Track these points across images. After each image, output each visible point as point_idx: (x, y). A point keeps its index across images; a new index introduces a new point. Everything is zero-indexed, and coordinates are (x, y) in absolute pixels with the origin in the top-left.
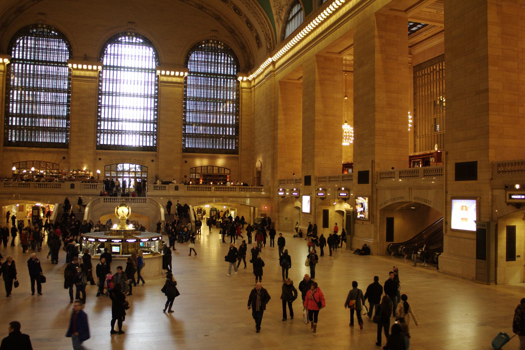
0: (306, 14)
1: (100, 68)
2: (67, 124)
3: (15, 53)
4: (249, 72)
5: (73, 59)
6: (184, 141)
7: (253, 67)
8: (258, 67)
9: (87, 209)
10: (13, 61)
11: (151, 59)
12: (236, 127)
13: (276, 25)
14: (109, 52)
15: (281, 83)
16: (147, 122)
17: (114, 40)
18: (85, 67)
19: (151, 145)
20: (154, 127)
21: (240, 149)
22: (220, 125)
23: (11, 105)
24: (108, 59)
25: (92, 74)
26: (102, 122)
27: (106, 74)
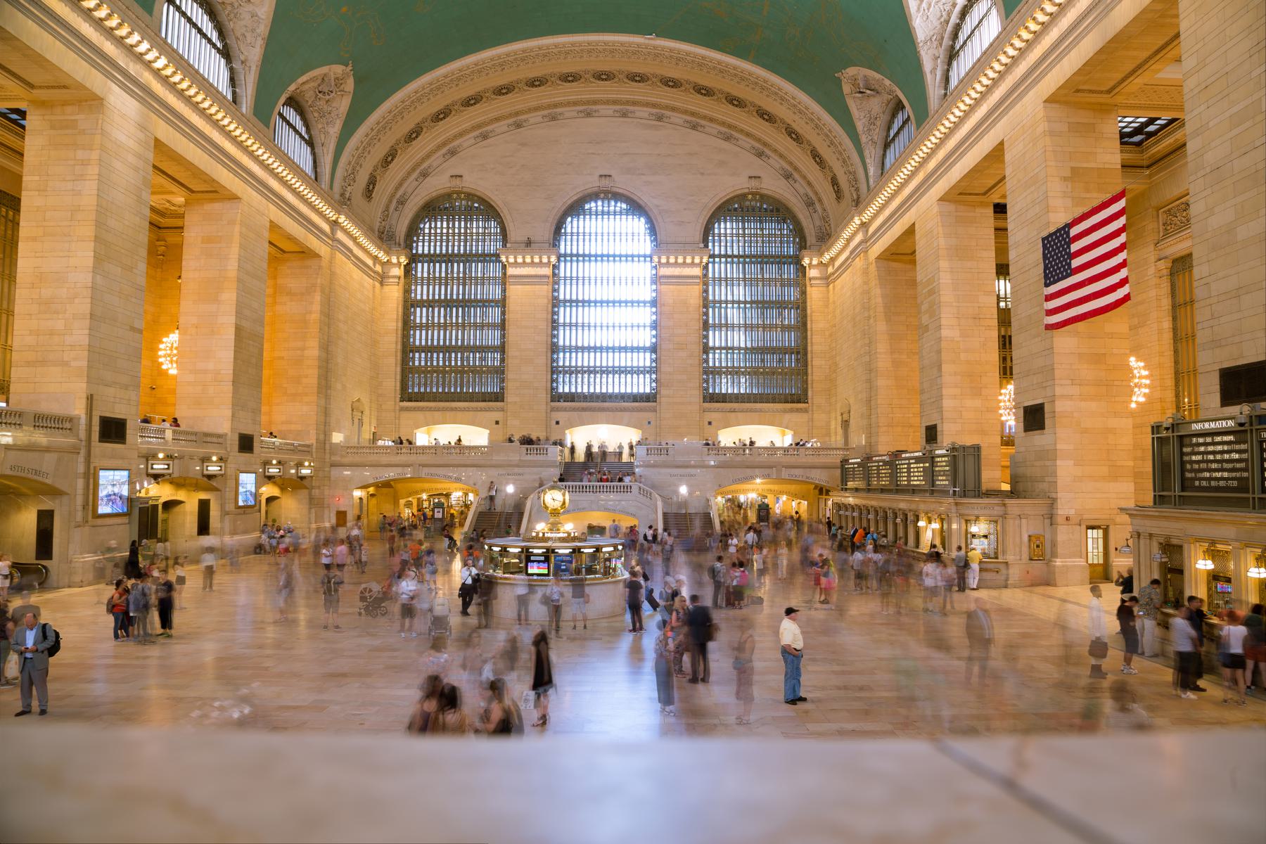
0: (919, 125)
2: (503, 360)
6: (707, 381)
7: (829, 235)
8: (837, 239)
10: (414, 259)
11: (642, 238)
13: (867, 153)
14: (569, 230)
15: (878, 258)
17: (576, 208)
19: (648, 390)
21: (810, 393)
24: (569, 243)
26: (561, 355)
27: (565, 269)
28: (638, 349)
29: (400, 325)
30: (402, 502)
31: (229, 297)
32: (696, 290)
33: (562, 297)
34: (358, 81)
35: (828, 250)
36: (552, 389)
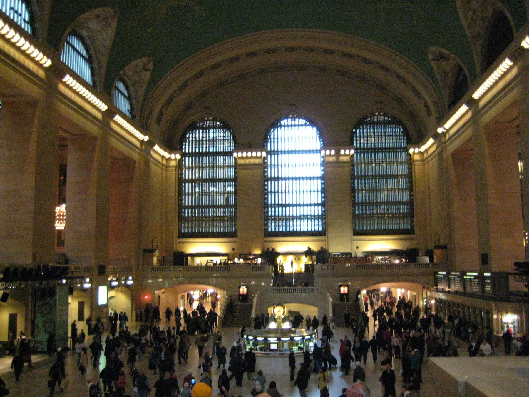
1: (264, 154)
3: (185, 148)
4: (421, 143)
5: (238, 147)
9: (255, 300)
10: (184, 155)
12: (411, 203)
16: (314, 205)
17: (276, 125)
18: (249, 154)
20: (322, 211)
22: (392, 203)
23: (183, 197)
24: (272, 144)
25: (257, 161)
26: (270, 209)
27: (271, 160)
28: (314, 205)
29: (177, 194)
30: (180, 296)
31: (93, 191)
32: (348, 169)
33: (269, 176)
34: (154, 64)
35: (423, 144)
36: (265, 229)
